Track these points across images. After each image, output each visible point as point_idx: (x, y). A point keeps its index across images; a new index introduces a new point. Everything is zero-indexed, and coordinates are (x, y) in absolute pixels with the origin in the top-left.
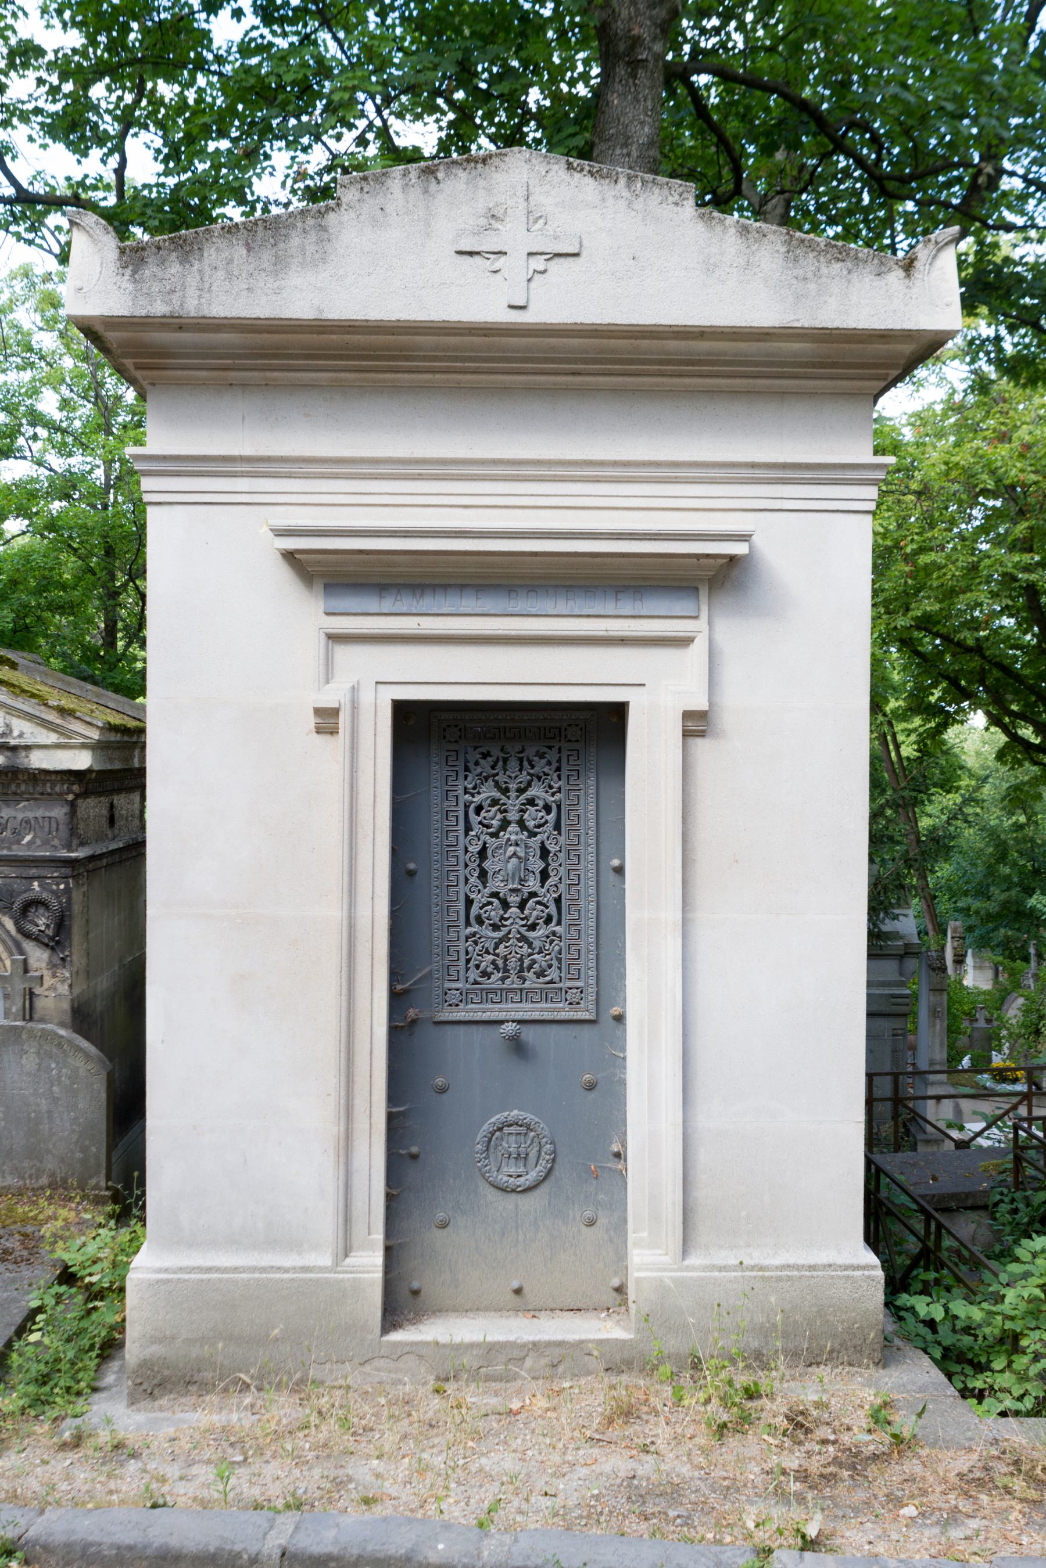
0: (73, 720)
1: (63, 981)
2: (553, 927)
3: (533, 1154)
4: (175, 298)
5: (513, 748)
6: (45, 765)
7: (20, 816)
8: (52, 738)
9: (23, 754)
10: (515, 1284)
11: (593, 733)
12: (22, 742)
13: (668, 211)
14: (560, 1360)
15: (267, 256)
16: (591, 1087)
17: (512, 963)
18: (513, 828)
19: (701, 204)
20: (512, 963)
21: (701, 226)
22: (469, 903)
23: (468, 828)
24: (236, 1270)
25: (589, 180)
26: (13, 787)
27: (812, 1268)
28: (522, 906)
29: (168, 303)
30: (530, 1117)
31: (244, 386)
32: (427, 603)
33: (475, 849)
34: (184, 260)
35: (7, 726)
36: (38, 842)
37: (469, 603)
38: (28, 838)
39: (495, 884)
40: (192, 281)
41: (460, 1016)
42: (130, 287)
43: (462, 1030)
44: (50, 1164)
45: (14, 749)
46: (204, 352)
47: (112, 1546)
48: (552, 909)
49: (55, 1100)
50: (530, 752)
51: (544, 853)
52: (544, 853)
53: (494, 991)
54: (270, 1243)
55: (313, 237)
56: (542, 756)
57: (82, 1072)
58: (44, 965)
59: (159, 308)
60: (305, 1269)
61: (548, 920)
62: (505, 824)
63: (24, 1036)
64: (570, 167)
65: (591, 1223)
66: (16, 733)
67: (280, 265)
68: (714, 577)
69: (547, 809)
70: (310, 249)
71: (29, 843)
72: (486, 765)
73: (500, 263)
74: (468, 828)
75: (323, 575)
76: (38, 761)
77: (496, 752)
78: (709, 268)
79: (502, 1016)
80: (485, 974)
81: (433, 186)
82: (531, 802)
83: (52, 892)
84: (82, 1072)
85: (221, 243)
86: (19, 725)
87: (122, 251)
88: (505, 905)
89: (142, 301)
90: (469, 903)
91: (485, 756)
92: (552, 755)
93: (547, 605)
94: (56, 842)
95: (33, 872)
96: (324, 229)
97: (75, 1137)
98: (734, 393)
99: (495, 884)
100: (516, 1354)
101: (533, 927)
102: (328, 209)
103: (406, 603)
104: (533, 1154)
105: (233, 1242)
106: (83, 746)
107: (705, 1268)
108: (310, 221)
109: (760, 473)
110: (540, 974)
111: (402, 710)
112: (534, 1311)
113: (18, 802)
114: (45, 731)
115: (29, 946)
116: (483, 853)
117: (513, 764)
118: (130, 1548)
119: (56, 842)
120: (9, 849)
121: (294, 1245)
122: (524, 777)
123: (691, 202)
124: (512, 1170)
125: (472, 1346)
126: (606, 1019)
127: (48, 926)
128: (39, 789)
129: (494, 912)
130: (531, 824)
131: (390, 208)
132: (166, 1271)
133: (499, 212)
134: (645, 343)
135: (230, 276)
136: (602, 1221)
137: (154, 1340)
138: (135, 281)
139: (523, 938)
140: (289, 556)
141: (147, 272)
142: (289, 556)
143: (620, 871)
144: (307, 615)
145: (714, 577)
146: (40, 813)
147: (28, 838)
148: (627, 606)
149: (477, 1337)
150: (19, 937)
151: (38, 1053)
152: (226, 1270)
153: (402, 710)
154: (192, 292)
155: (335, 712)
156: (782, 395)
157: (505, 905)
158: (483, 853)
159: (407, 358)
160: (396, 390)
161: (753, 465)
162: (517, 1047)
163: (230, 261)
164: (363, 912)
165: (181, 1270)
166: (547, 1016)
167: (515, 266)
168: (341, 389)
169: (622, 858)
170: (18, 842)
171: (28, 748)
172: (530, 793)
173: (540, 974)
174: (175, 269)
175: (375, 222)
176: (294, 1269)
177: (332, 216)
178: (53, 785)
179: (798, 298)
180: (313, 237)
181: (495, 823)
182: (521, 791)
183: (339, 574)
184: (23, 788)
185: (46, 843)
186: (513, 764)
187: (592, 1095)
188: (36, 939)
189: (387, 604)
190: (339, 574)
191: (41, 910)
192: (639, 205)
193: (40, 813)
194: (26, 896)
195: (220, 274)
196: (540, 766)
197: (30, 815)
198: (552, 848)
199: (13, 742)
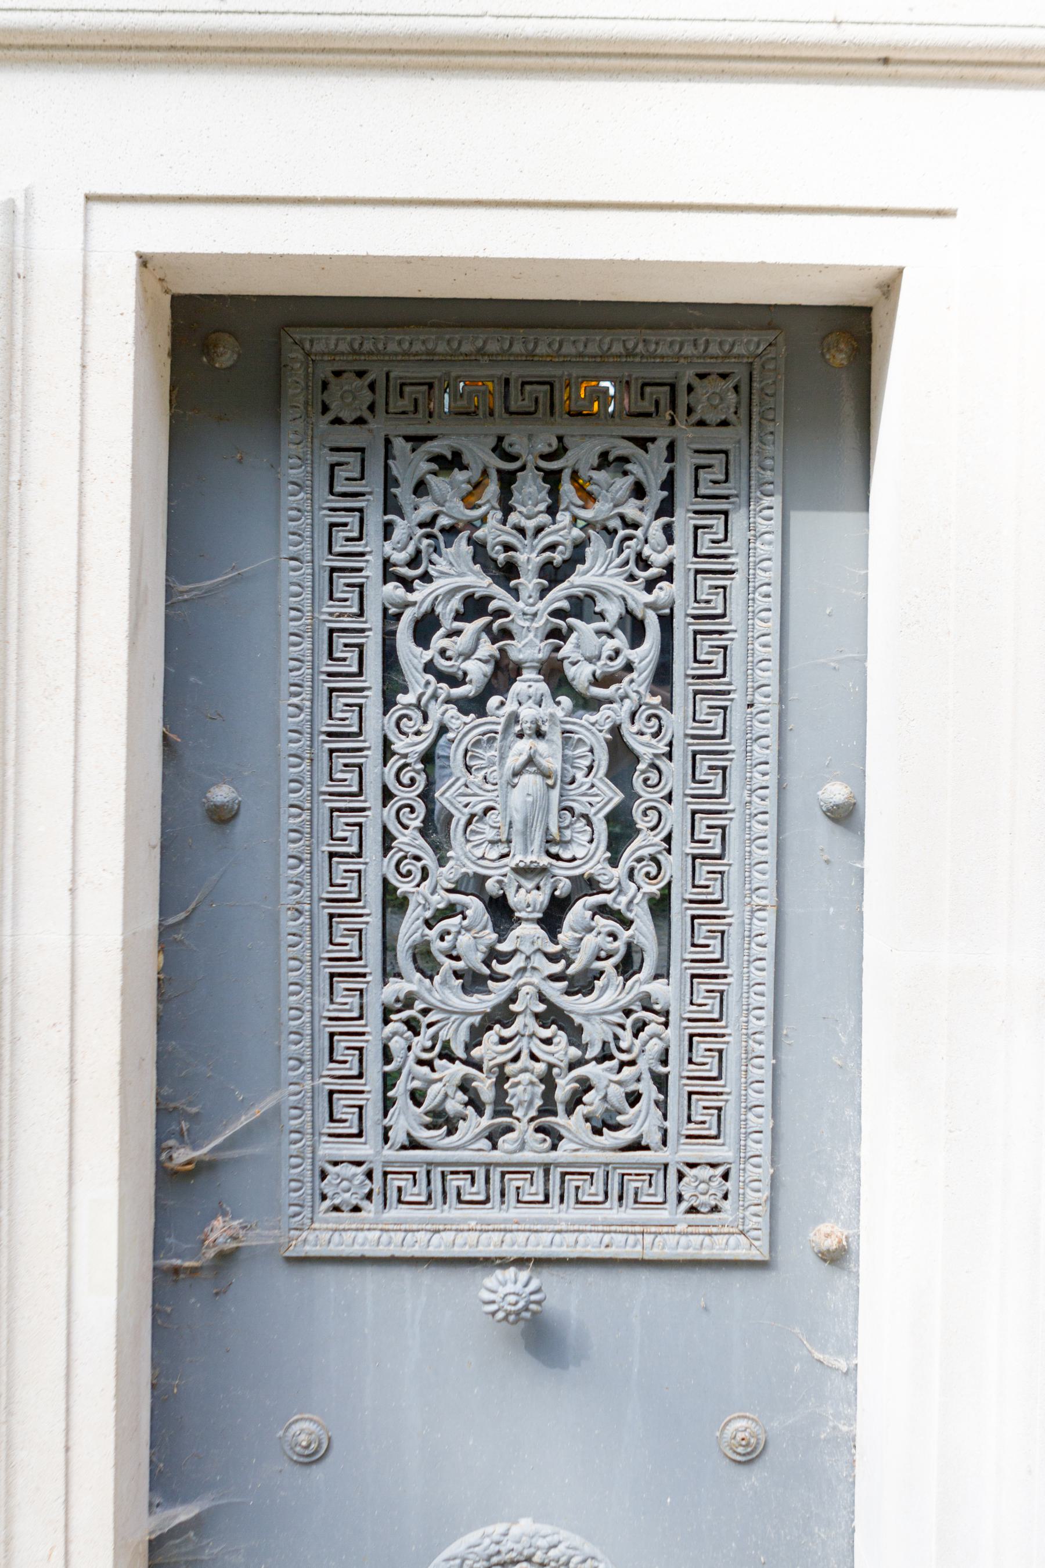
2: (642, 983)
5: (531, 442)
16: (749, 1457)
17: (524, 1091)
18: (529, 684)
20: (524, 1091)
28: (552, 918)
33: (409, 747)
43: (371, 1276)
48: (644, 929)
51: (621, 758)
52: (621, 758)
61: (628, 966)
62: (504, 673)
77: (480, 454)
79: (488, 1245)
80: (442, 1120)
88: (501, 912)
90: (393, 902)
92: (649, 467)
99: (466, 855)
101: (583, 984)
110: (603, 1125)
117: (530, 490)
129: (471, 937)
130: (580, 674)
139: (551, 1015)
143: (846, 816)
157: (501, 912)
162: (538, 1335)
172: (579, 581)
181: (477, 670)
182: (553, 574)
186: (530, 490)
187: (752, 1479)
198: (645, 747)
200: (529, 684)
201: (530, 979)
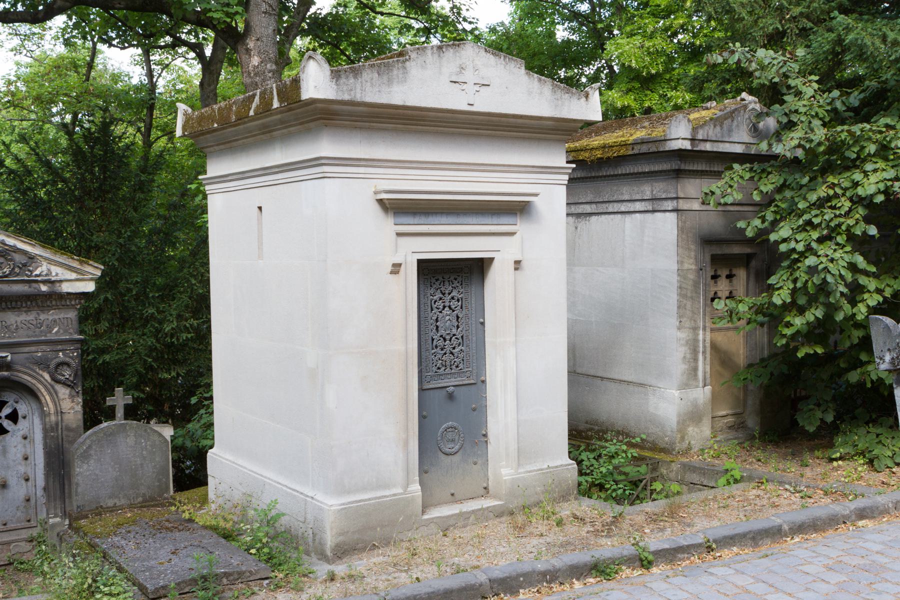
0: (86, 266)
1: (78, 404)
2: (460, 347)
3: (457, 438)
4: (352, 93)
5: (446, 276)
6: (70, 290)
7: (51, 318)
8: (74, 276)
9: (58, 284)
10: (453, 491)
11: (475, 269)
12: (58, 278)
13: (516, 70)
14: (481, 515)
15: (385, 78)
16: (474, 410)
17: (448, 363)
18: (447, 309)
19: (526, 68)
20: (448, 363)
21: (527, 77)
22: (433, 340)
23: (432, 310)
24: (369, 499)
25: (492, 56)
26: (48, 303)
27: (557, 467)
29: (350, 95)
30: (455, 424)
31: (361, 128)
32: (431, 219)
33: (434, 318)
34: (355, 77)
35: (49, 270)
36: (61, 331)
37: (444, 219)
38: (56, 329)
39: (442, 332)
40: (358, 86)
41: (431, 386)
42: (336, 87)
43: (432, 391)
44: (143, 490)
45: (53, 282)
46: (350, 114)
47: (425, 594)
48: (460, 340)
49: (144, 458)
50: (452, 278)
51: (458, 317)
52: (458, 317)
53: (442, 375)
54: (379, 487)
55: (401, 71)
56: (456, 279)
57: (157, 443)
58: (67, 396)
59: (346, 97)
60: (395, 495)
61: (459, 345)
62: (444, 307)
63: (128, 428)
64: (486, 51)
65: (475, 464)
66: (54, 274)
67: (390, 82)
68: (518, 209)
69: (458, 300)
70: (401, 76)
71: (56, 332)
72: (437, 283)
73: (465, 86)
74: (432, 310)
75: (392, 209)
76: (66, 288)
77: (441, 279)
78: (530, 93)
79: (445, 385)
80: (439, 368)
81: (442, 54)
82: (453, 298)
83: (70, 357)
84: (157, 443)
85: (369, 71)
86: (55, 270)
87: (332, 71)
88: (445, 340)
89: (340, 93)
90: (433, 340)
91: (437, 280)
92: (459, 279)
93: (469, 220)
94: (71, 331)
95: (60, 347)
96: (405, 68)
97: (154, 475)
98: (524, 138)
99: (442, 332)
100: (467, 516)
101: (454, 348)
102: (406, 60)
103: (423, 219)
104: (457, 438)
105: (364, 489)
106: (91, 279)
107: (524, 473)
108: (400, 65)
109: (535, 170)
110: (457, 367)
111: (420, 262)
112: (460, 501)
113: (49, 311)
114: (69, 272)
115: (58, 387)
116: (437, 320)
117: (447, 283)
118: (433, 593)
119: (71, 331)
120: (46, 336)
121: (386, 486)
122: (450, 288)
123: (523, 68)
124: (450, 446)
125: (452, 515)
126: (480, 383)
127: (70, 375)
128: (63, 303)
129: (441, 343)
130: (453, 307)
131: (427, 62)
132: (344, 504)
133: (464, 66)
134: (503, 119)
135: (372, 85)
136: (480, 462)
137: (340, 534)
138: (337, 85)
139: (451, 353)
140: (380, 201)
141: (343, 80)
142: (380, 201)
143: (483, 324)
144: (388, 225)
145: (518, 209)
146: (62, 316)
147: (56, 329)
148: (495, 220)
149: (457, 511)
150: (53, 383)
151: (135, 436)
152: (366, 500)
153: (420, 262)
154: (358, 90)
155: (400, 265)
156: (539, 139)
157: (445, 340)
158: (437, 320)
159: (424, 121)
160: (416, 132)
161: (533, 167)
162: (451, 396)
163: (372, 79)
164: (410, 346)
165: (349, 503)
166: (461, 383)
167: (470, 88)
168: (395, 130)
169: (484, 319)
170: (50, 332)
171: (61, 281)
172: (452, 295)
173: (457, 367)
174: (352, 80)
175: (422, 67)
176: (390, 496)
177: (408, 63)
178: (71, 300)
179: (556, 106)
180: (401, 71)
181: (441, 307)
182: (449, 294)
183: (398, 208)
184: (54, 303)
185: (66, 331)
186: (447, 283)
187: (475, 413)
188: (64, 384)
189: (417, 220)
190: (398, 208)
191: (65, 367)
192: (508, 67)
193: (62, 316)
194: (57, 360)
195: (369, 84)
196: (456, 284)
197: (57, 317)
198: (461, 316)
199: (53, 279)
200: (447, 309)
201: (448, 349)
